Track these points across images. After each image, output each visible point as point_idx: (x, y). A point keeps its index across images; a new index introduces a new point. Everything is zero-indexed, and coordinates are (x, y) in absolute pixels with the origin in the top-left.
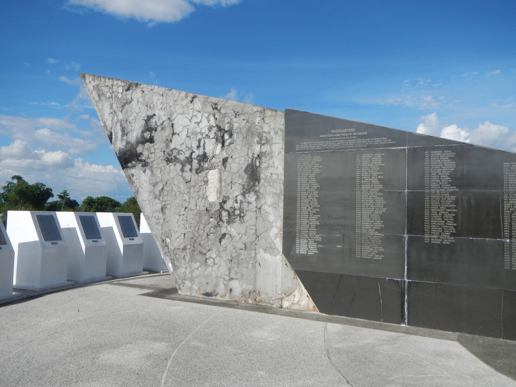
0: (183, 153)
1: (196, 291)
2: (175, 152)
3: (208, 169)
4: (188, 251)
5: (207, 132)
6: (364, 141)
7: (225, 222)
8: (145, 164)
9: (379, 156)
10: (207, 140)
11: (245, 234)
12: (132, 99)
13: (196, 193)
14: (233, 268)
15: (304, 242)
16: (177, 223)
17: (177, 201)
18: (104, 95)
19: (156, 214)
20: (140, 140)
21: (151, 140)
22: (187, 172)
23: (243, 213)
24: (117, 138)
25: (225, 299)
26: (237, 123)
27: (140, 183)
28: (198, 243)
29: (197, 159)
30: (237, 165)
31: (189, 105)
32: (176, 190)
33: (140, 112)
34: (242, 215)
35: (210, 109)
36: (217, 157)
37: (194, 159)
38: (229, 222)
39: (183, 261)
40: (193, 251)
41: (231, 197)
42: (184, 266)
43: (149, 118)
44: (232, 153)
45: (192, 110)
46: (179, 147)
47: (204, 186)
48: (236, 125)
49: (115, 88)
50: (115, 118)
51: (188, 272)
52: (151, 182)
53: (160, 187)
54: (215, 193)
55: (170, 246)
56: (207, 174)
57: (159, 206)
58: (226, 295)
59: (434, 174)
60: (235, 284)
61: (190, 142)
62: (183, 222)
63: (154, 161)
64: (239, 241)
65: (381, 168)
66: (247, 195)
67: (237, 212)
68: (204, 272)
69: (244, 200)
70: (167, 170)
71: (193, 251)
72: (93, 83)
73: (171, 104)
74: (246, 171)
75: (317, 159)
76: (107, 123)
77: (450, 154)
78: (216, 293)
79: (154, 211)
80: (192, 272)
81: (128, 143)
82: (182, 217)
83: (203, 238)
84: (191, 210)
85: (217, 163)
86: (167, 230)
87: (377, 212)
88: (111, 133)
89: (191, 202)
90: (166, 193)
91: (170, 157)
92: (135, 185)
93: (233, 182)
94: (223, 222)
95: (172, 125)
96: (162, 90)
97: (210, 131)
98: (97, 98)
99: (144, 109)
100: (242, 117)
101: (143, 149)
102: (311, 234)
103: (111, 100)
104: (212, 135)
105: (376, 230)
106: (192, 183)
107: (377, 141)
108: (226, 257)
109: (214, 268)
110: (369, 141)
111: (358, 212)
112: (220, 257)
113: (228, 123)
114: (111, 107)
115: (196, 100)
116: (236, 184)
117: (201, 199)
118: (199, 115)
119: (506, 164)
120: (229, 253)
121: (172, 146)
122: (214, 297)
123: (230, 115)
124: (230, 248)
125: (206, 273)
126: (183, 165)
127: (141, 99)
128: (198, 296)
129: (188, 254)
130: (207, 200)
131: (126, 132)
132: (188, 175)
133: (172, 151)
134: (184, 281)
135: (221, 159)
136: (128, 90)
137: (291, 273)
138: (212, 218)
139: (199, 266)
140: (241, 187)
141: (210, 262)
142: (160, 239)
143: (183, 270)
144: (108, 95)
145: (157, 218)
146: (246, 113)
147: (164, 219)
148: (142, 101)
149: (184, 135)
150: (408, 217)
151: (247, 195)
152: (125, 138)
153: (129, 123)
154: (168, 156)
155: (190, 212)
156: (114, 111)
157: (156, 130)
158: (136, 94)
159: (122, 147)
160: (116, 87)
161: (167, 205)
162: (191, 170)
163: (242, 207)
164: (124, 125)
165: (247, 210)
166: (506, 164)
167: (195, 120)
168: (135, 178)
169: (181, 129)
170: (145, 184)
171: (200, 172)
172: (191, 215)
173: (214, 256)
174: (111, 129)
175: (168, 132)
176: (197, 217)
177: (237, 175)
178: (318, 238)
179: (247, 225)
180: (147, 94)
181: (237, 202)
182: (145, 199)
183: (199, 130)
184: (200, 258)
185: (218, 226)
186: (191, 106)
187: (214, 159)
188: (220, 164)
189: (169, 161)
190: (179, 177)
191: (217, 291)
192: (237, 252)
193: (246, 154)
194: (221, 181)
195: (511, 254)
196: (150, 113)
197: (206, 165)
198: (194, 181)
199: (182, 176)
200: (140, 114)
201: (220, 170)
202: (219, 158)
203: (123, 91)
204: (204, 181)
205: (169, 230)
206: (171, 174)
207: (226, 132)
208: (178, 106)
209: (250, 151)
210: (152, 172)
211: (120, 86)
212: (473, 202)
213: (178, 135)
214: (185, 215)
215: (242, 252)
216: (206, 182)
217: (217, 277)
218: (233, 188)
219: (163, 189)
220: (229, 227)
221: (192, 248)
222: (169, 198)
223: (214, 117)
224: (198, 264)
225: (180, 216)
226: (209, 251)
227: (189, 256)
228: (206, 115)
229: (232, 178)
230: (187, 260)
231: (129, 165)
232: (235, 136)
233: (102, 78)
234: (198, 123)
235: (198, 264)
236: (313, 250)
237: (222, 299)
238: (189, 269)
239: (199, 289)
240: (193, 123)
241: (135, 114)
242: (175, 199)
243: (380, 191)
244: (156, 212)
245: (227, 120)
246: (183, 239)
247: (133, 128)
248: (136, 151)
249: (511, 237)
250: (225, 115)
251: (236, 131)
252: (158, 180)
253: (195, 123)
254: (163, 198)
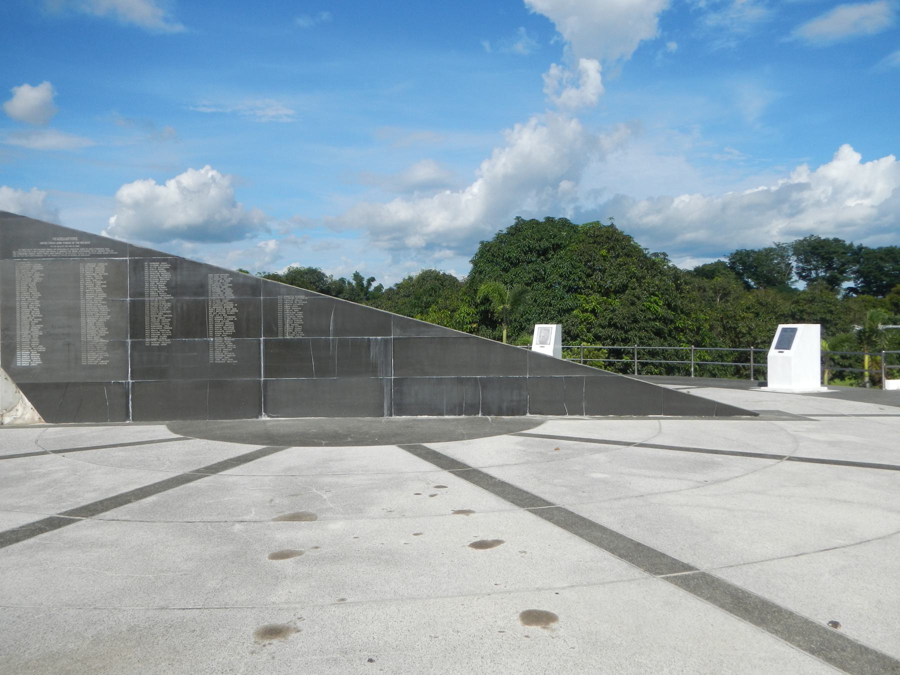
6: (87, 250)
9: (102, 266)
15: (25, 353)
59: (152, 284)
65: (105, 278)
75: (39, 266)
77: (166, 265)
87: (101, 320)
102: (33, 345)
105: (101, 337)
107: (100, 251)
110: (92, 250)
111: (83, 320)
119: (210, 275)
137: (12, 387)
150: (131, 323)
166: (210, 275)
178: (42, 349)
195: (214, 350)
212: (185, 307)
236: (36, 361)
243: (104, 299)
249: (214, 337)
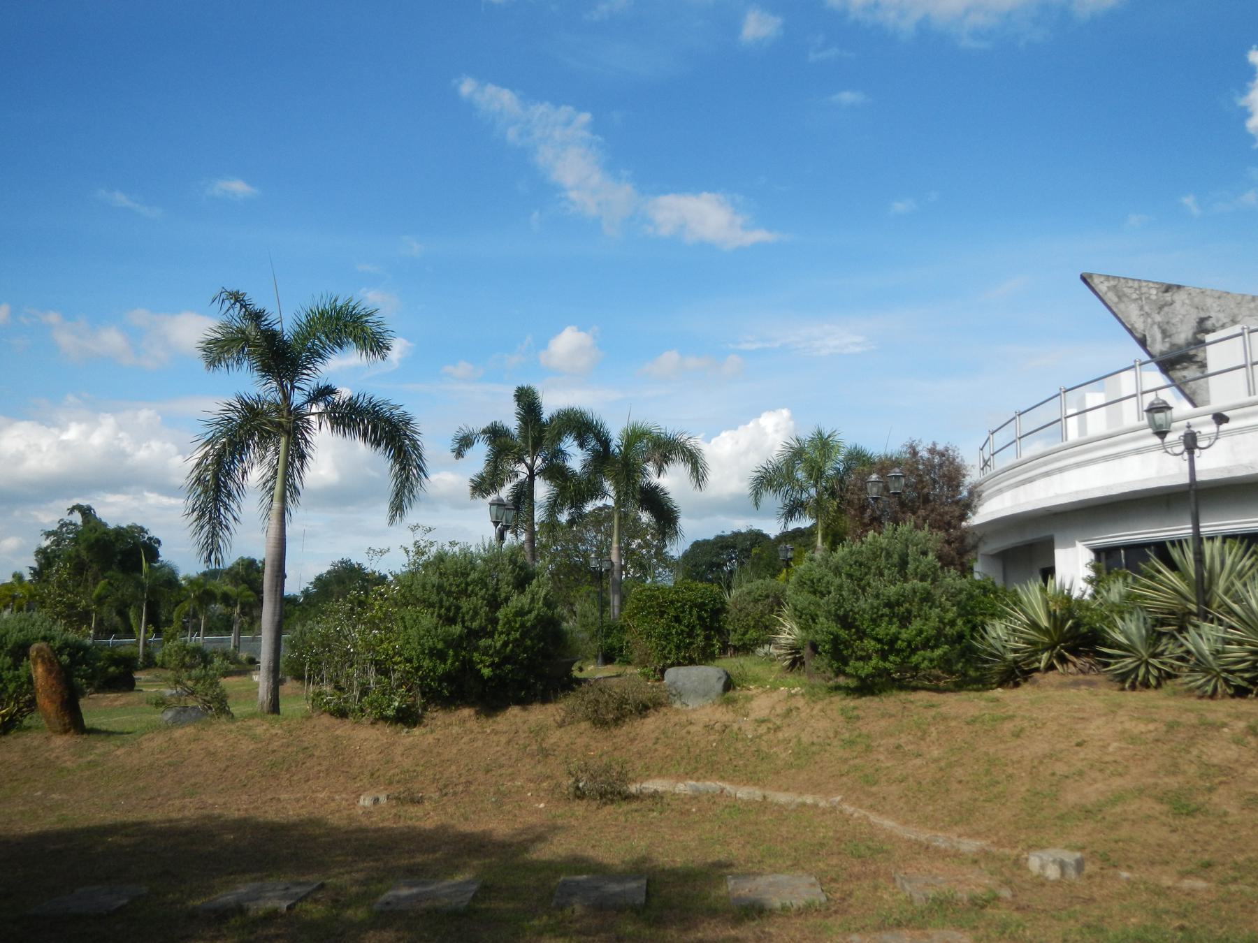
24: (1154, 341)
43: (1202, 321)
49: (1144, 290)
72: (1106, 284)
81: (1173, 345)
98: (1116, 300)
99: (1193, 311)
114: (1141, 308)
136: (1167, 291)
144: (1135, 296)
158: (1180, 297)
164: (1165, 326)
196: (1203, 315)
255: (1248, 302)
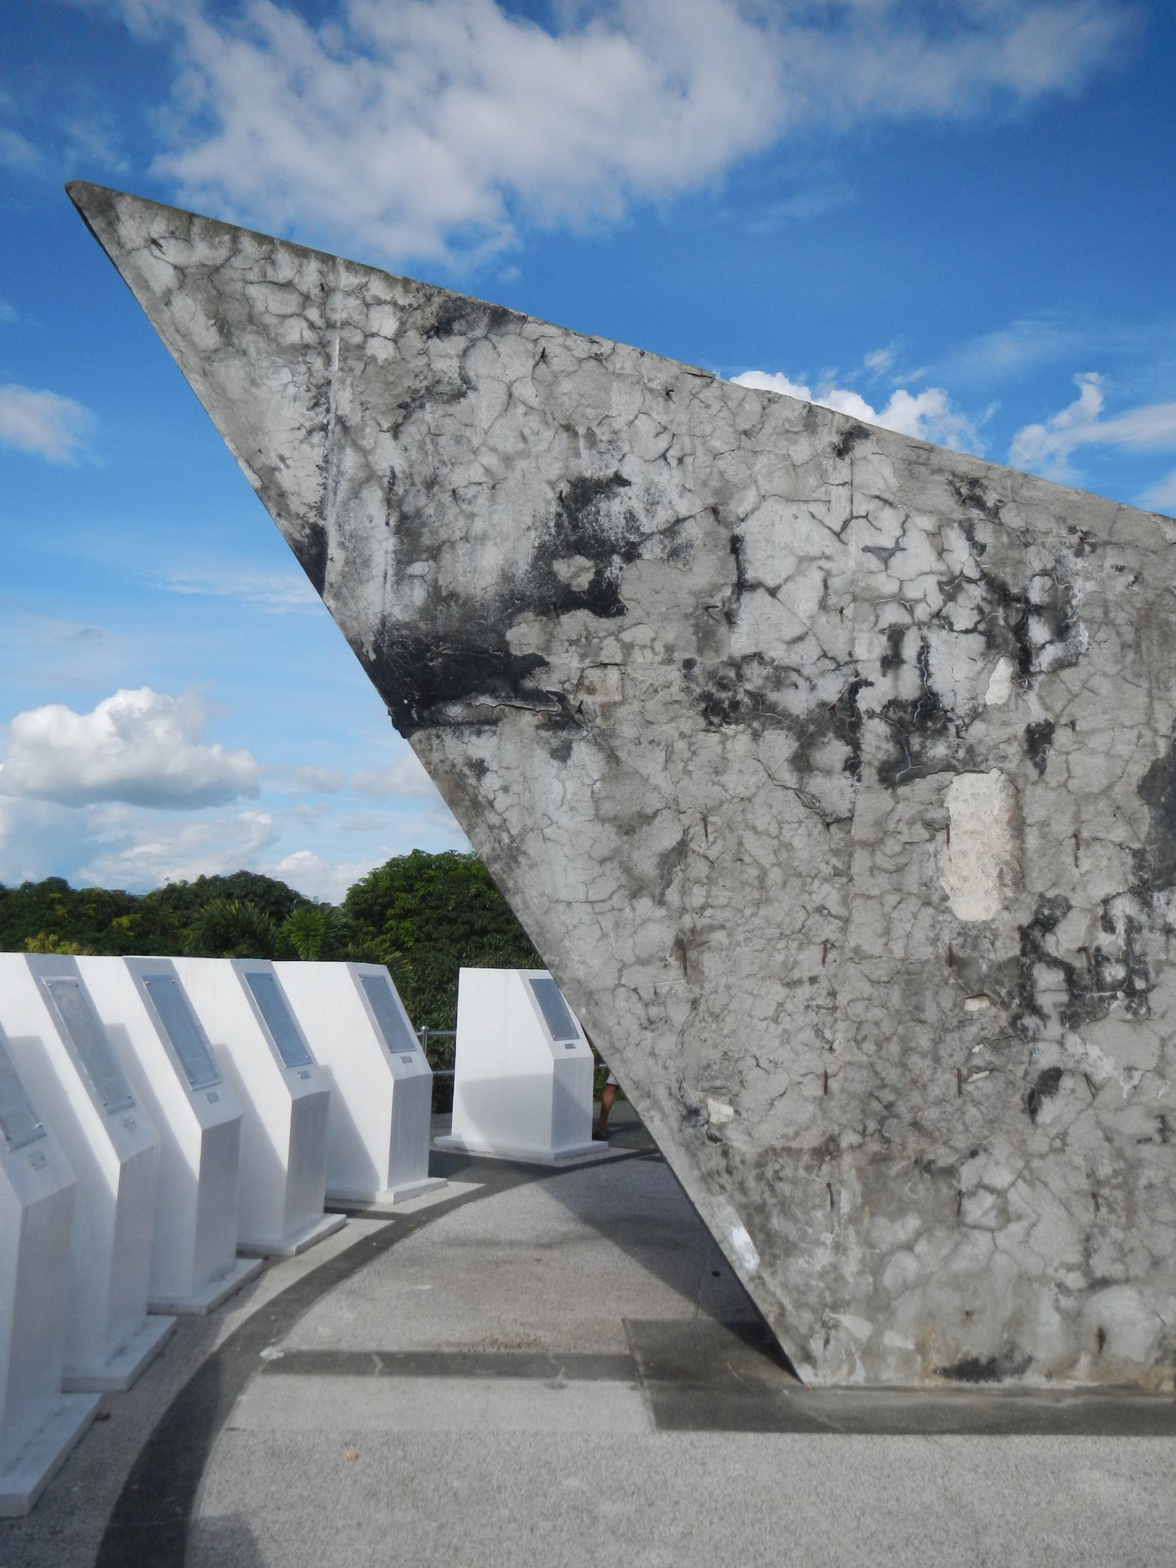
0: (801, 682)
1: (906, 1358)
2: (756, 676)
3: (948, 767)
4: (847, 1160)
5: (936, 600)
7: (1054, 1015)
8: (564, 719)
10: (936, 638)
11: (1160, 1073)
12: (465, 380)
13: (883, 880)
14: (1103, 1231)
16: (776, 1020)
17: (775, 912)
18: (264, 331)
19: (640, 977)
20: (530, 590)
21: (604, 600)
22: (828, 773)
23: (1145, 975)
24: (358, 564)
25: (1070, 1384)
26: (1087, 579)
27: (529, 810)
28: (908, 1117)
29: (884, 715)
30: (1100, 761)
31: (828, 463)
32: (767, 859)
33: (524, 454)
34: (1140, 984)
35: (941, 498)
36: (997, 717)
37: (872, 715)
38: (1072, 1018)
39: (819, 1214)
40: (880, 1160)
41: (1077, 900)
42: (828, 1238)
43: (582, 493)
44: (1073, 708)
45: (844, 492)
46: (777, 653)
47: (931, 848)
48: (1082, 589)
49: (343, 307)
50: (350, 461)
51: (850, 1268)
52: (608, 808)
53: (665, 836)
54: (991, 883)
55: (737, 1139)
56: (941, 789)
57: (661, 936)
58: (1072, 1363)
60: (1120, 1308)
61: (842, 636)
62: (812, 1017)
63: (615, 704)
64: (1129, 1103)
66: (1159, 899)
67: (1115, 972)
68: (947, 1260)
69: (1143, 918)
70: (704, 756)
71: (880, 1160)
72: (173, 252)
73: (717, 444)
74: (1146, 789)
76: (286, 479)
78: (1018, 1358)
79: (629, 957)
80: (876, 1266)
81: (439, 597)
82: (806, 991)
83: (935, 1091)
84: (859, 955)
85: (996, 746)
86: (715, 1055)
88: (318, 535)
89: (858, 917)
90: (699, 868)
91: (723, 695)
92: (493, 819)
93: (1085, 834)
94: (1044, 1018)
95: (736, 545)
96: (661, 373)
97: (951, 597)
98: (208, 337)
99: (550, 441)
100: (1112, 558)
101: (550, 638)
103: (318, 363)
104: (963, 615)
106: (860, 830)
108: (1066, 1179)
109: (1002, 1239)
112: (1031, 1183)
113: (1044, 573)
114: (320, 396)
115: (861, 448)
116: (1097, 847)
117: (912, 904)
118: (889, 519)
120: (1079, 1160)
121: (739, 642)
122: (1008, 1382)
123: (1050, 540)
124: (1084, 1135)
125: (960, 1265)
126: (807, 735)
127: (527, 391)
128: (916, 1383)
129: (851, 1175)
130: (948, 910)
131: (426, 540)
132: (835, 790)
133: (737, 664)
134: (828, 1314)
135: (1020, 730)
136: (441, 329)
138: (980, 995)
139: (919, 1234)
140: (1130, 861)
141: (978, 1209)
142: (668, 1104)
143: (823, 1258)
144: (296, 332)
145: (647, 994)
146: (1128, 543)
147: (695, 1003)
148: (535, 402)
149: (804, 596)
151: (1159, 899)
152: (418, 568)
153: (447, 499)
154: (711, 688)
155: (852, 969)
156: (340, 420)
157: (631, 554)
159: (399, 614)
160: (353, 302)
161: (712, 928)
162: (852, 766)
163: (1137, 948)
164: (416, 501)
165: (1160, 966)
167: (860, 535)
168: (490, 783)
169: (786, 567)
170: (564, 819)
171: (907, 780)
172: (854, 986)
173: (1000, 1177)
174: (320, 508)
175: (706, 571)
176: (895, 997)
177: (1102, 804)
179: (1165, 1029)
180: (569, 374)
181: (1109, 927)
182: (564, 895)
183: (891, 588)
184: (922, 1190)
185: (1016, 1032)
186: (841, 471)
187: (978, 730)
188: (1014, 751)
189: (717, 711)
190: (780, 794)
191: (1026, 1346)
192: (1120, 1154)
193: (1143, 718)
194: (1018, 825)
196: (589, 466)
197: (939, 750)
198: (870, 818)
199: (799, 792)
200: (522, 465)
201: (1012, 779)
202: (1005, 724)
203: (401, 333)
204: (928, 825)
205: (726, 1056)
206: (730, 779)
207: (1038, 610)
208: (762, 460)
209: (1157, 705)
210: (612, 758)
211: (380, 302)
213: (773, 592)
214: (824, 983)
215: (1147, 1151)
216: (939, 828)
217: (1024, 1279)
218: (1085, 865)
219: (681, 849)
220: (1073, 1041)
221: (874, 1146)
222: (721, 896)
223: (970, 537)
224: (913, 1222)
225: (791, 984)
226: (974, 1154)
227: (858, 1187)
228: (928, 522)
229: (1077, 819)
230: (845, 1206)
231: (455, 711)
232: (1083, 634)
233: (246, 243)
234: (885, 555)
235: (913, 1222)
237: (1054, 1384)
238: (856, 1252)
239: (921, 1348)
240: (854, 549)
241: (491, 460)
242: (758, 904)
244: (644, 962)
245: (1036, 560)
246: (820, 1102)
247: (478, 526)
248: (504, 646)
250: (1025, 538)
251: (1085, 613)
252: (654, 802)
253: (866, 549)
254: (684, 892)
255: (788, 434)
